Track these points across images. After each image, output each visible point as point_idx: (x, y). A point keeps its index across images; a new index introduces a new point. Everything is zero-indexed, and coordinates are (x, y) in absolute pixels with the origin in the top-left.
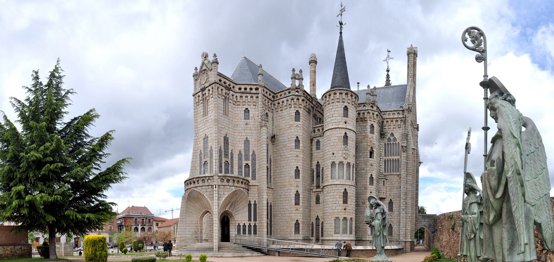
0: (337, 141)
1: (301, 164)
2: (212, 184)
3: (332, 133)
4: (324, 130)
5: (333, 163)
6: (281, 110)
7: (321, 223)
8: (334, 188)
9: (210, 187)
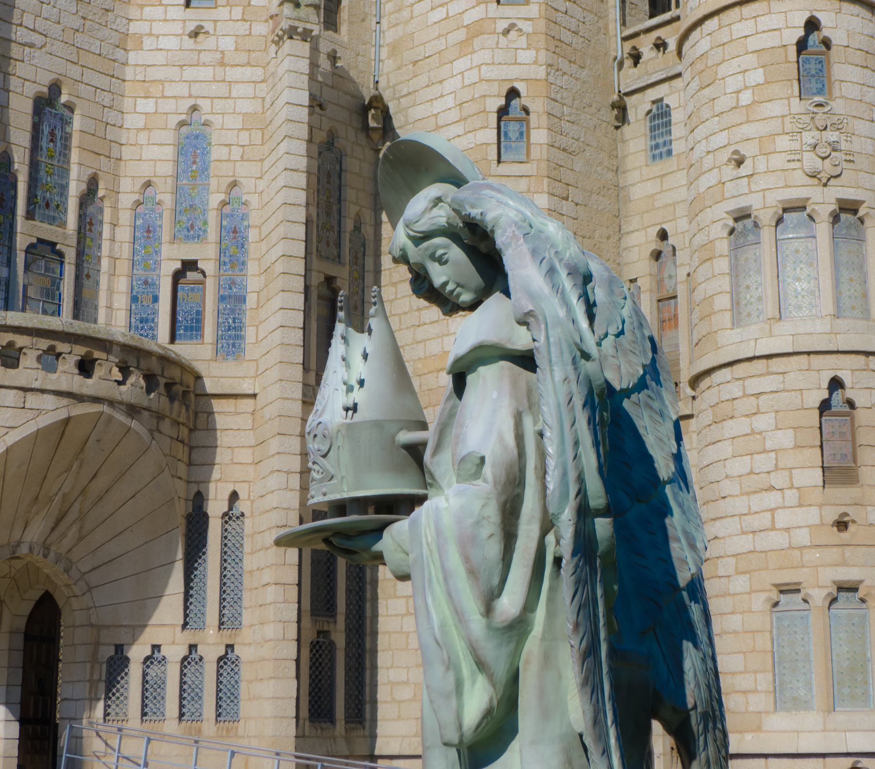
0: (758, 76)
8: (754, 386)
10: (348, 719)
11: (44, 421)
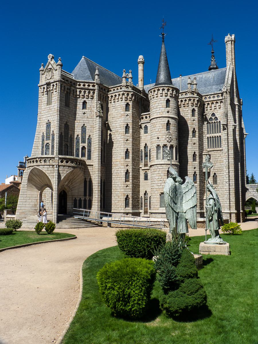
0: (161, 127)
1: (131, 146)
2: (54, 164)
3: (156, 121)
4: (151, 118)
5: (158, 146)
6: (114, 102)
7: (149, 197)
8: (159, 168)
9: (51, 166)
10: (103, 208)
11: (71, 170)
